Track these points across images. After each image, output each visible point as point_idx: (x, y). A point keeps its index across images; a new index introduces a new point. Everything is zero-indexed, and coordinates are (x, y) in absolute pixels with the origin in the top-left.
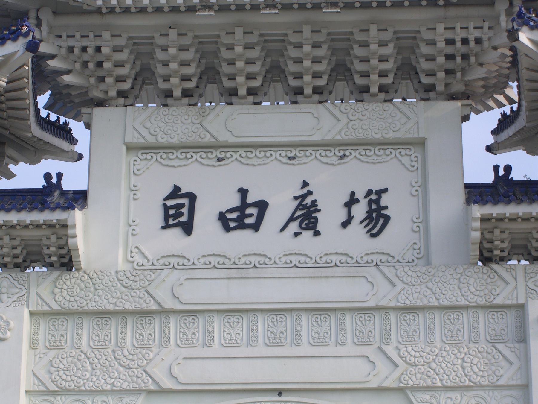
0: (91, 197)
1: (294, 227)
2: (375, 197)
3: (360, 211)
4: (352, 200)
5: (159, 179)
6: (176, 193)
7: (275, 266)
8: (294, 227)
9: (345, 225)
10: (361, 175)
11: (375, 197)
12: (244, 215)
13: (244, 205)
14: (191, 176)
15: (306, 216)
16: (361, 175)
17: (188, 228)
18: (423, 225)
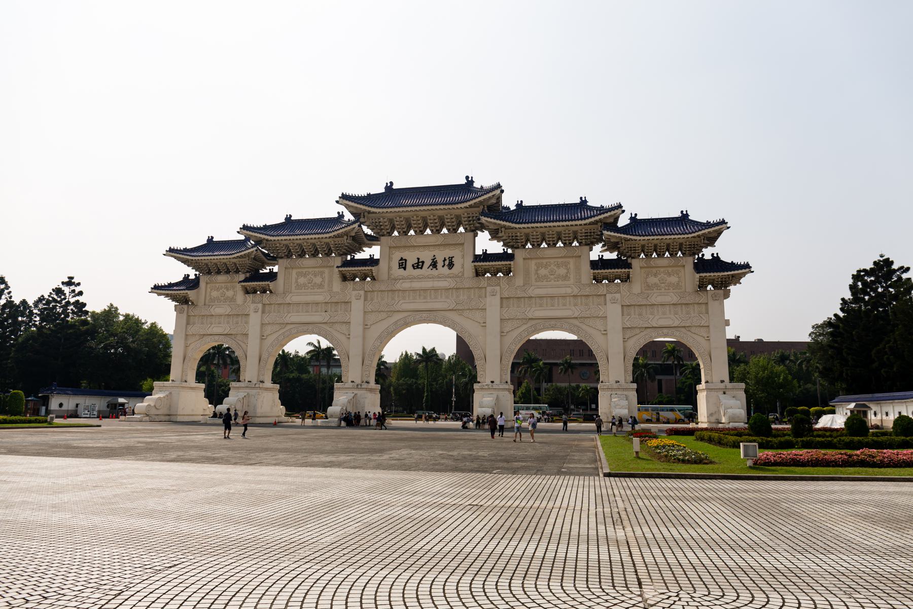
2: (451, 259)
3: (447, 262)
4: (445, 260)
6: (402, 259)
7: (426, 279)
11: (451, 259)
12: (419, 265)
15: (434, 265)
17: (405, 268)
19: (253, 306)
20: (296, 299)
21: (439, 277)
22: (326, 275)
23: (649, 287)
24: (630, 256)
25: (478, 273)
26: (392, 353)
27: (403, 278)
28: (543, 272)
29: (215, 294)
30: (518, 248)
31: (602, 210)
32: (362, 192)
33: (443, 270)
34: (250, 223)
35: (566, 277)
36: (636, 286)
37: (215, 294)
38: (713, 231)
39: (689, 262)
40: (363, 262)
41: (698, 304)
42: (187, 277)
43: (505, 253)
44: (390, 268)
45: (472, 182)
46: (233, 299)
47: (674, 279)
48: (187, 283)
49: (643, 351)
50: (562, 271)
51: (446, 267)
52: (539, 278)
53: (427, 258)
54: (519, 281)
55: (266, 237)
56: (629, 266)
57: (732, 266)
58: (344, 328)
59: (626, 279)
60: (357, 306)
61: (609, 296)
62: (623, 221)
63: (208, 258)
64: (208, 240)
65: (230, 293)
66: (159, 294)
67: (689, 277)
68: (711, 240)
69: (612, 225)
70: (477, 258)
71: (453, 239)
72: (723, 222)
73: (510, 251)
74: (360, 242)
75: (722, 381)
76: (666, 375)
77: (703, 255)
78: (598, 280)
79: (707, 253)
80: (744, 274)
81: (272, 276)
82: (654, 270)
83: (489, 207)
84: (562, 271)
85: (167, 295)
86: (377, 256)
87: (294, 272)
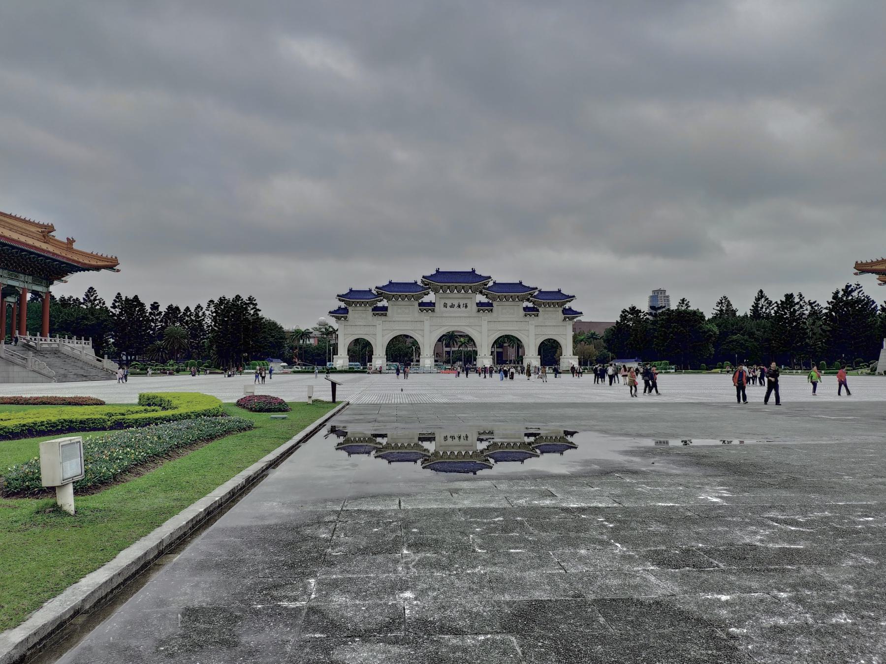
10: (465, 301)
12: (452, 306)
15: (459, 306)
16: (465, 301)
19: (379, 321)
25: (479, 311)
33: (463, 309)
39: (561, 309)
42: (340, 308)
53: (456, 303)
54: (494, 314)
56: (538, 311)
58: (420, 332)
65: (364, 316)
71: (467, 296)
79: (567, 306)
81: (385, 309)
86: (433, 301)
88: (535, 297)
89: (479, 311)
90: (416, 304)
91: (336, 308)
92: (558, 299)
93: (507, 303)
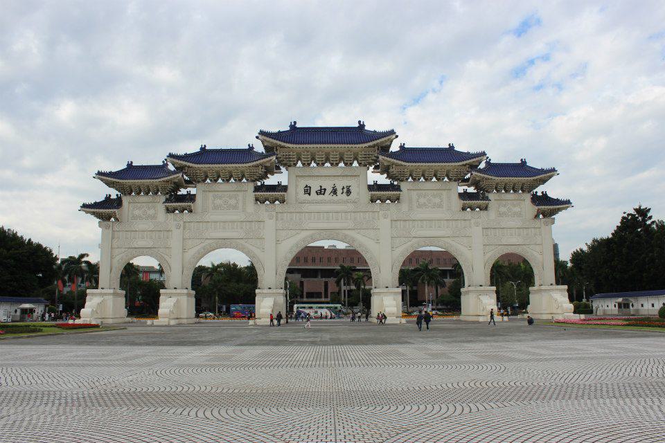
0: (289, 187)
1: (332, 194)
2: (348, 187)
3: (345, 190)
4: (343, 188)
5: (303, 183)
6: (307, 186)
8: (332, 194)
9: (342, 193)
11: (348, 187)
12: (321, 191)
13: (321, 190)
14: (310, 182)
15: (334, 192)
17: (309, 194)
18: (358, 194)
20: (214, 218)
21: (338, 202)
22: (240, 198)
23: (501, 215)
24: (487, 191)
25: (373, 200)
26: (206, 262)
27: (309, 202)
28: (422, 200)
29: (137, 212)
30: (402, 181)
31: (467, 156)
32: (275, 130)
33: (341, 196)
34: (174, 152)
35: (440, 206)
36: (492, 214)
37: (137, 212)
38: (546, 175)
39: (528, 197)
40: (272, 188)
41: (534, 228)
42: (108, 198)
43: (392, 184)
44: (296, 193)
45: (364, 126)
46: (154, 217)
47: (517, 209)
48: (108, 202)
49: (409, 260)
50: (437, 200)
51: (344, 194)
52: (420, 206)
54: (404, 206)
55: (188, 164)
56: (487, 199)
57: (557, 202)
59: (486, 208)
60: (270, 225)
61: (473, 221)
62: (482, 166)
63: (130, 179)
64: (128, 165)
65: (151, 212)
66: (87, 212)
67: (526, 207)
68: (543, 181)
69: (473, 167)
70: (371, 188)
71: (348, 171)
72: (554, 170)
73: (396, 183)
74: (269, 171)
75: (551, 284)
76: (512, 279)
77: (536, 192)
78: (464, 209)
79: (539, 190)
80: (566, 208)
81: (191, 198)
82: (504, 202)
83: (382, 147)
84: (437, 200)
85: (93, 213)
86: (284, 183)
87: (211, 194)
88: (480, 171)
89: (373, 200)
90: (251, 186)
91: (102, 198)
92: (522, 177)
93: (428, 185)
